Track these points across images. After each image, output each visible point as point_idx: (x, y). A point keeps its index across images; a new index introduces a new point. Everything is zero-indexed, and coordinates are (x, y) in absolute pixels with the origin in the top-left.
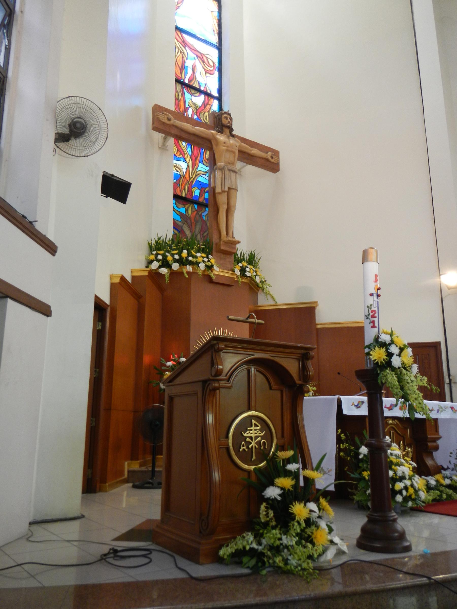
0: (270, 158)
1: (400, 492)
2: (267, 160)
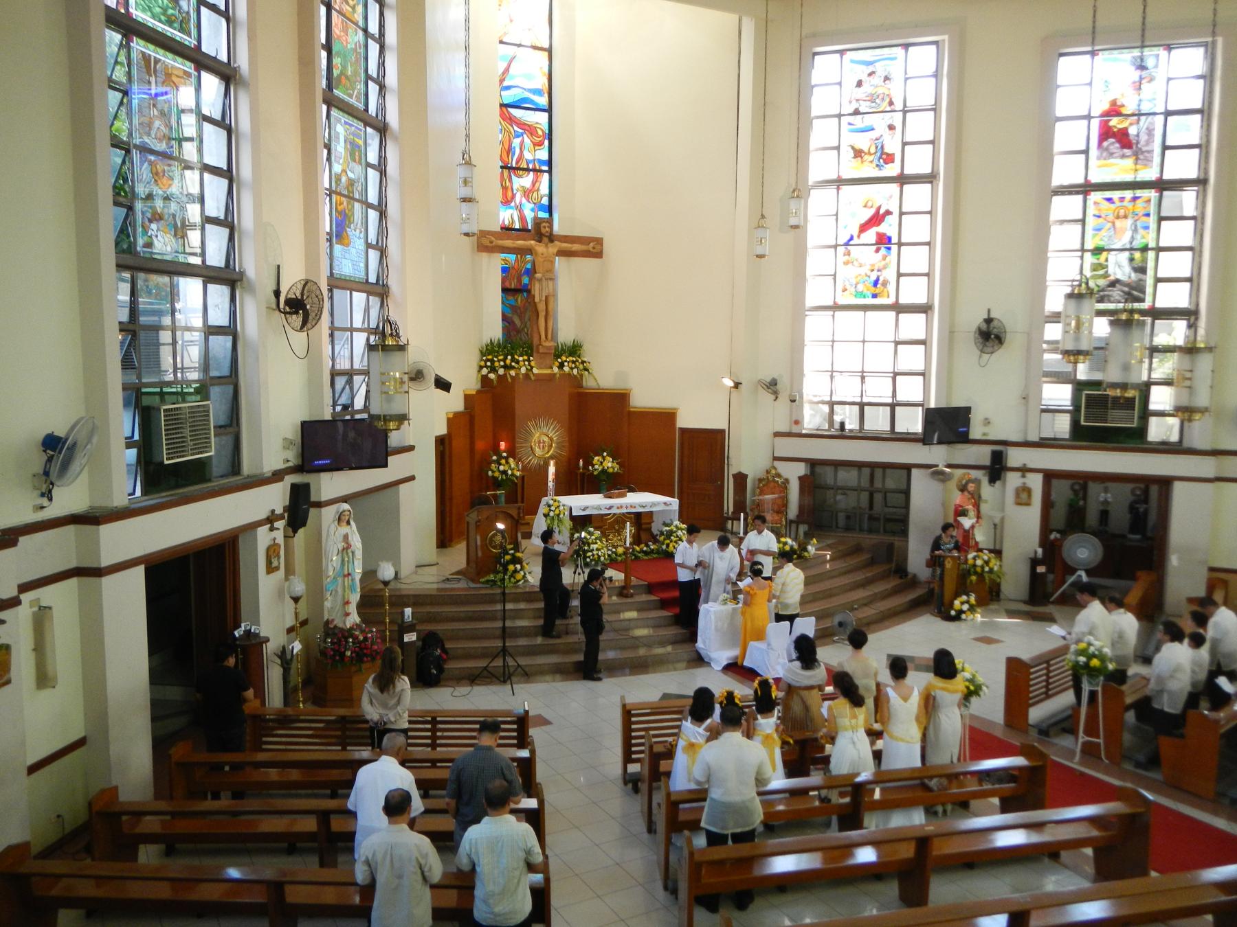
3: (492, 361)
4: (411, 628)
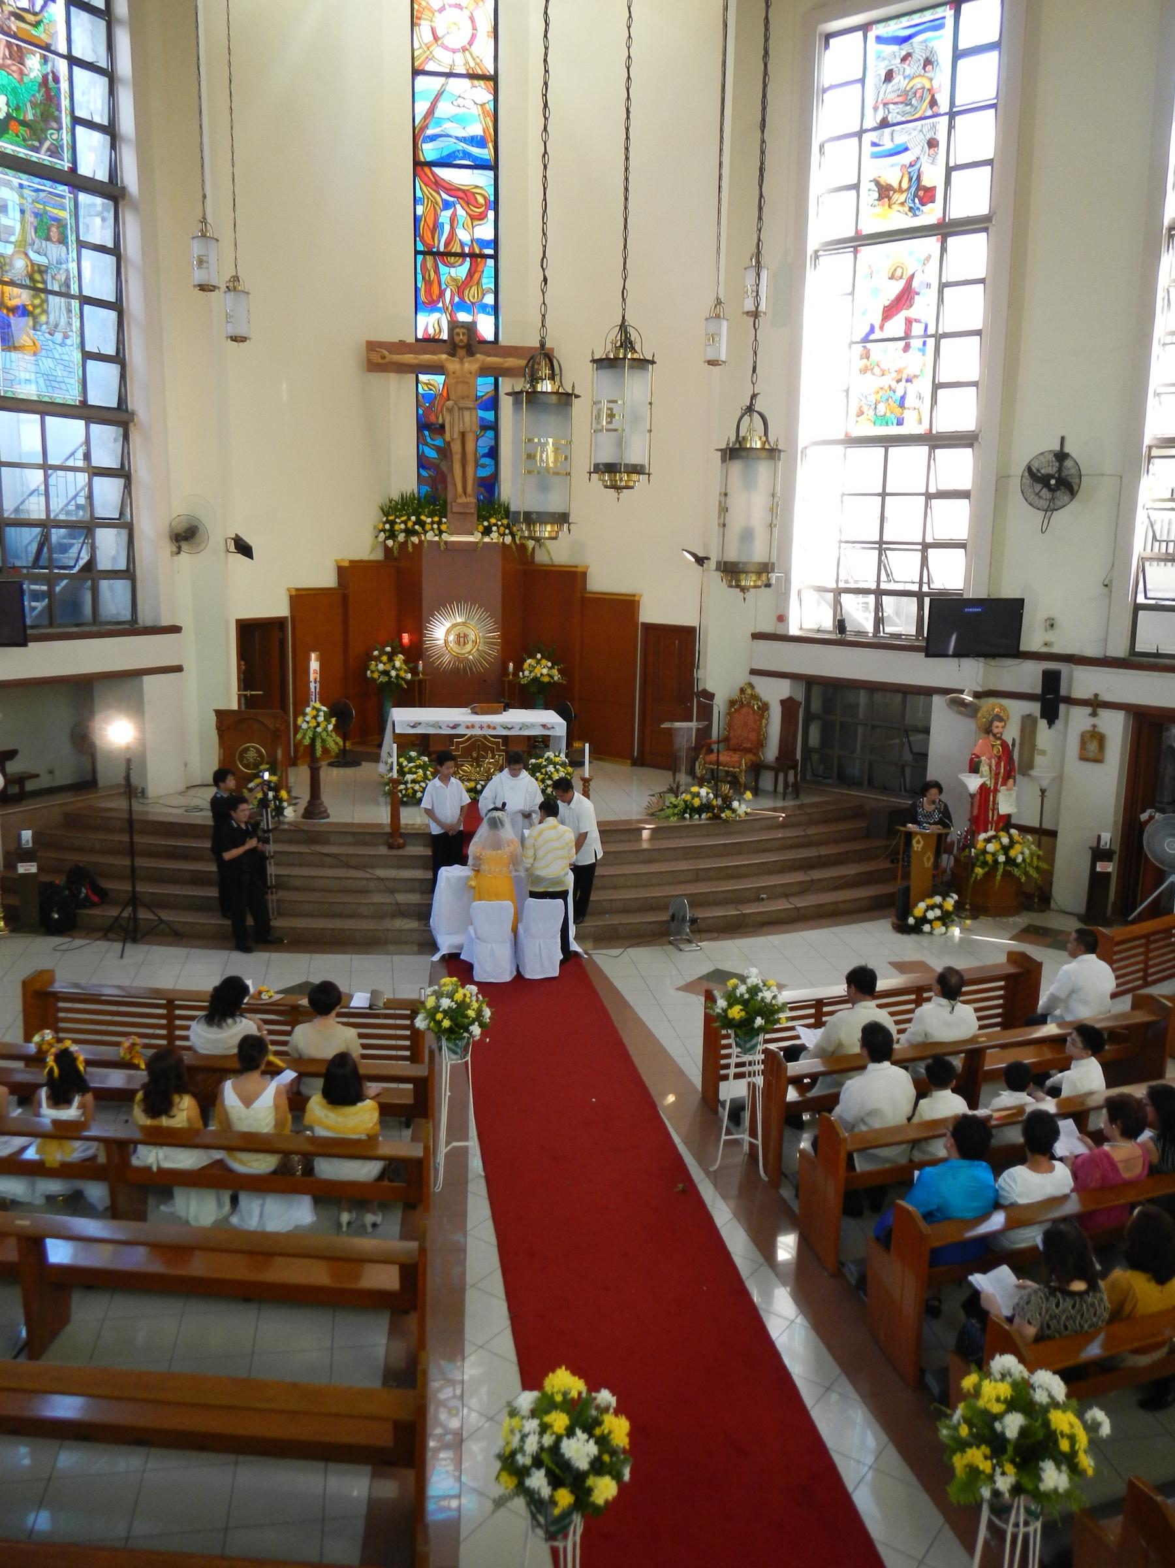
1: (401, 791)
3: (392, 523)
4: (27, 856)
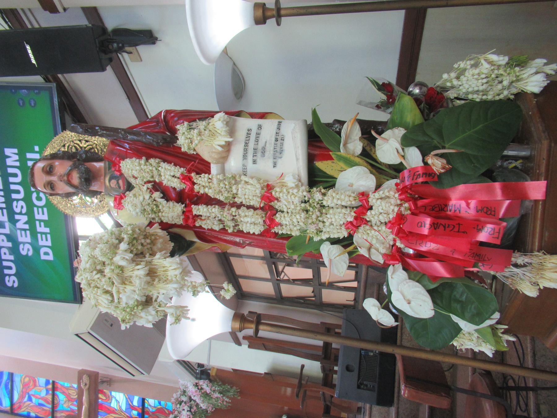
0: (87, 386)
2: (89, 389)
